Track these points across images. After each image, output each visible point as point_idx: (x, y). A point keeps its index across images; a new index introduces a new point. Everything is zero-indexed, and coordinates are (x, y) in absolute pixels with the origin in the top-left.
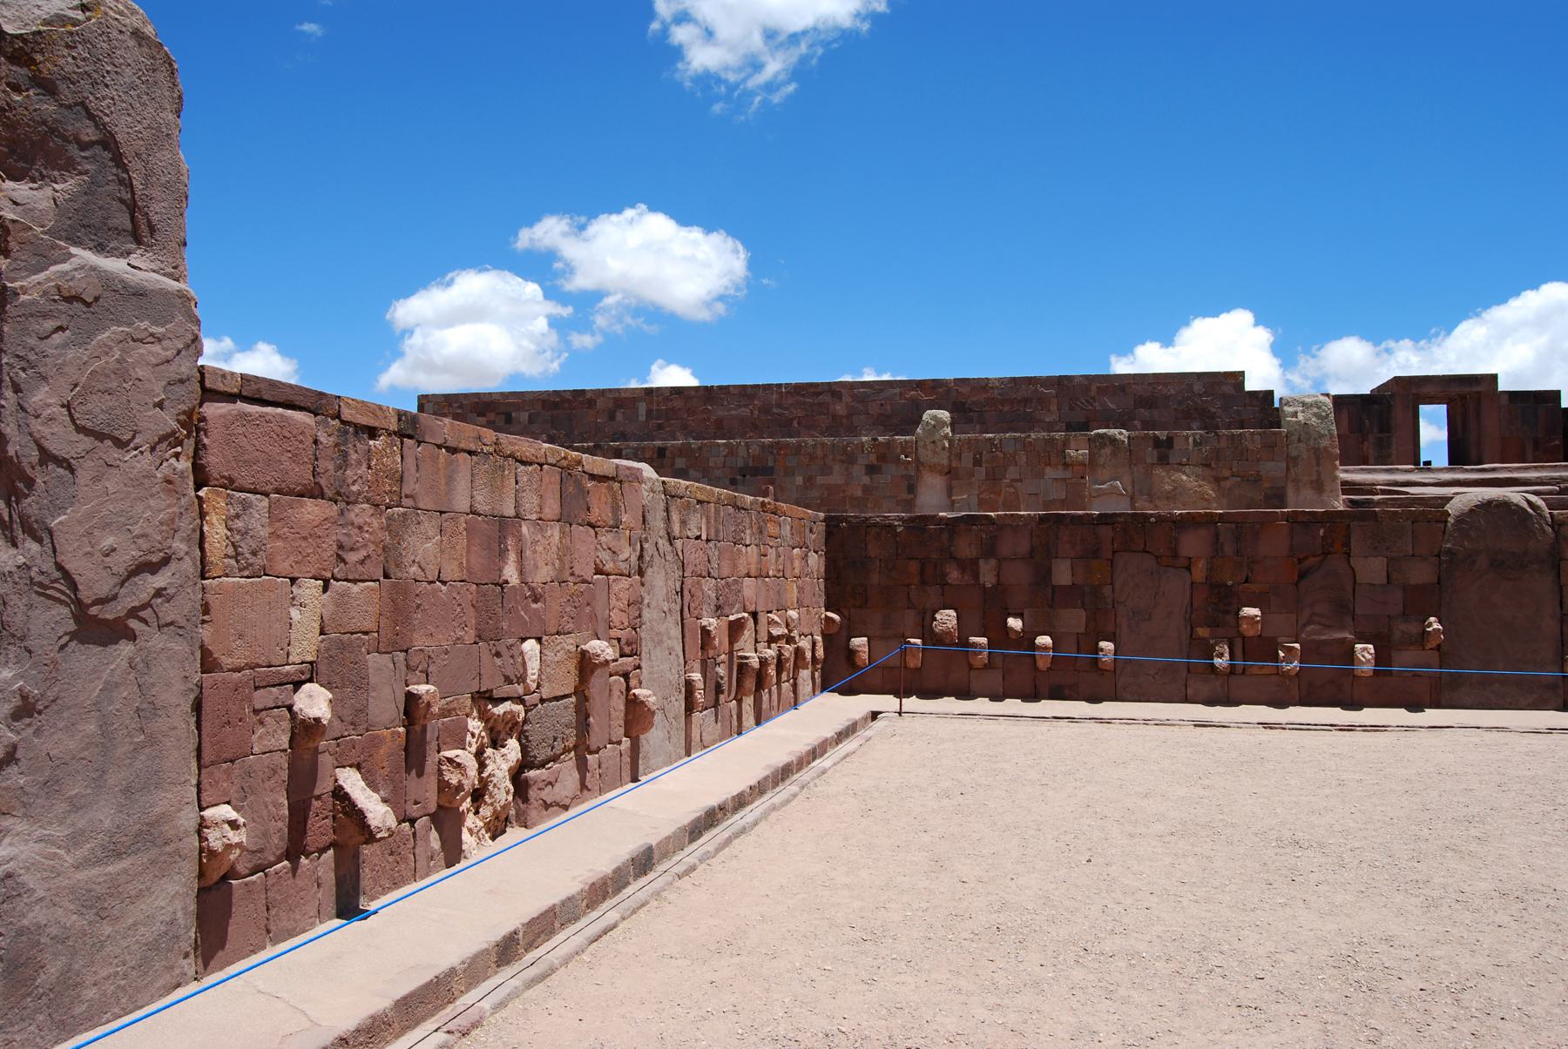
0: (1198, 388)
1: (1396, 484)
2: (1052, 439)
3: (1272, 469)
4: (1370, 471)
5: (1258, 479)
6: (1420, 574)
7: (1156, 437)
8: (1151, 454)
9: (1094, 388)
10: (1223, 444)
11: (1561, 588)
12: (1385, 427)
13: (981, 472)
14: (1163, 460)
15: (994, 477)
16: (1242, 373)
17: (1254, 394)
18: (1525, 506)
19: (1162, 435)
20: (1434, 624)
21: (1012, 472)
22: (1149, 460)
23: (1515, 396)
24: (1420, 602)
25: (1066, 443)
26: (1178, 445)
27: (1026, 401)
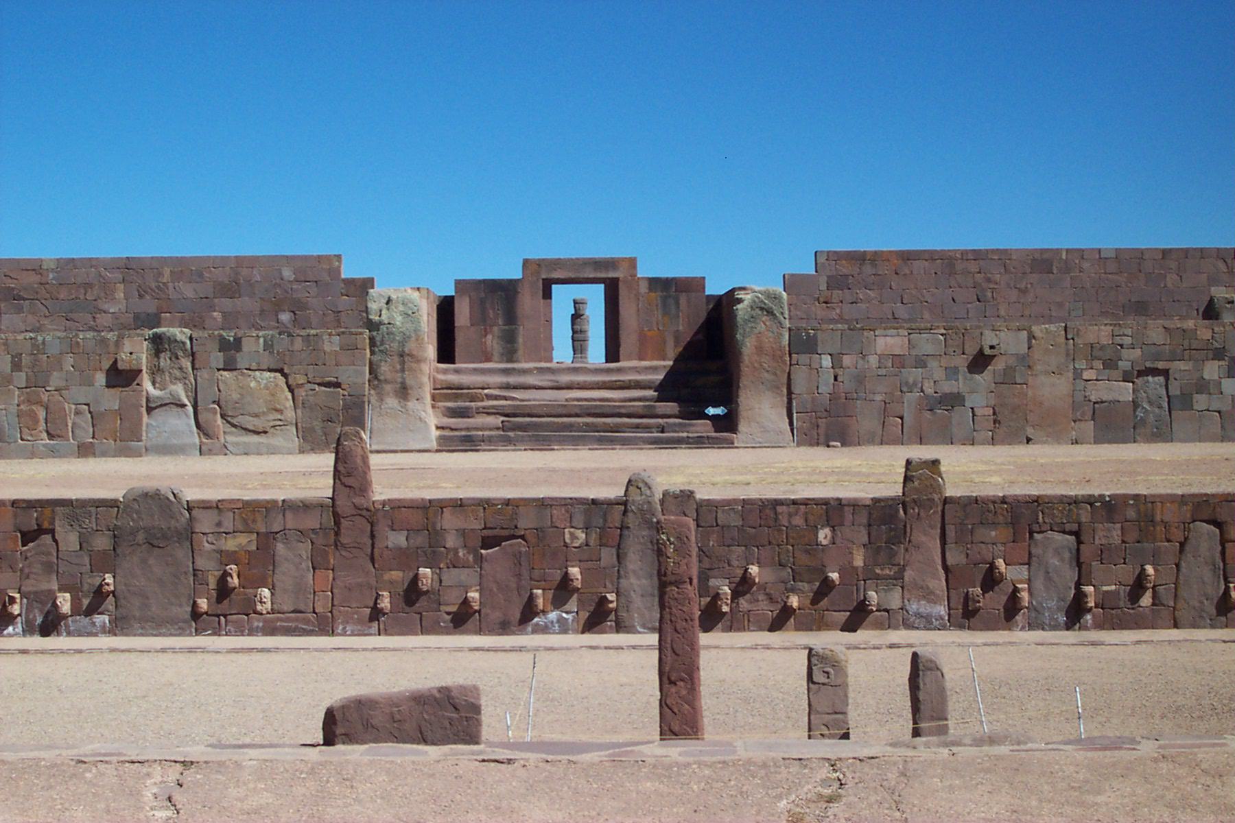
0: (287, 273)
1: (508, 387)
2: (104, 341)
3: (355, 375)
4: (483, 372)
5: (337, 385)
6: (102, 543)
7: (221, 336)
8: (217, 358)
9: (167, 271)
10: (298, 344)
12: (511, 317)
13: (21, 378)
14: (229, 366)
15: (37, 382)
16: (339, 257)
17: (350, 282)
19: (230, 336)
20: (109, 579)
21: (56, 380)
22: (214, 365)
23: (654, 283)
24: (103, 562)
25: (118, 344)
26: (248, 345)
27: (88, 286)
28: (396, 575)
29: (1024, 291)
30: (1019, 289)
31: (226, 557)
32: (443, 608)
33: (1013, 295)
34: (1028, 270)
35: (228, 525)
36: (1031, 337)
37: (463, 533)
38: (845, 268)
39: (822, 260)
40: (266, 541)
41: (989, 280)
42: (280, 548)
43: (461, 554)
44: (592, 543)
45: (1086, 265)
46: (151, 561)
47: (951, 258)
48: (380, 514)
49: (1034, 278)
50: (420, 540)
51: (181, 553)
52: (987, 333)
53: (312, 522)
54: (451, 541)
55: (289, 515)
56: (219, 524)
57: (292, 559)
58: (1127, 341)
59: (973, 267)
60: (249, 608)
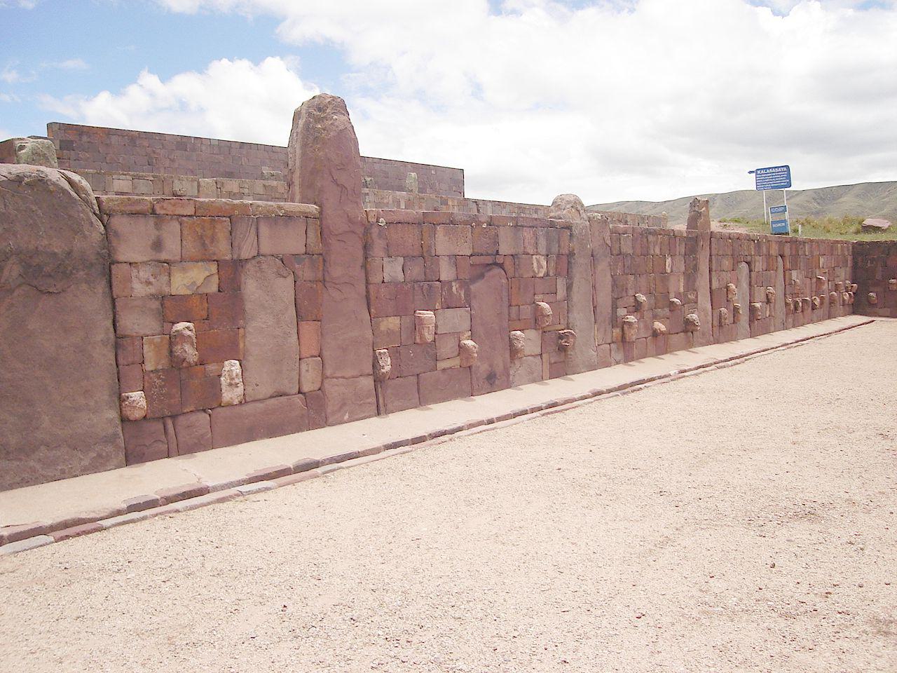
11: (113, 301)
18: (67, 186)
28: (392, 323)
29: (173, 161)
30: (170, 160)
31: (169, 307)
32: (441, 365)
33: (167, 163)
34: (174, 148)
35: (172, 248)
36: (199, 186)
37: (455, 259)
38: (70, 136)
39: (56, 128)
40: (231, 272)
41: (154, 152)
42: (251, 287)
43: (454, 289)
44: (551, 274)
45: (204, 148)
46: (33, 324)
47: (132, 136)
48: (375, 231)
49: (178, 153)
50: (416, 271)
51: (89, 300)
52: (176, 181)
53: (293, 242)
54: (446, 272)
55: (264, 230)
56: (158, 245)
57: (268, 300)
58: (246, 191)
59: (146, 143)
60: (210, 398)
